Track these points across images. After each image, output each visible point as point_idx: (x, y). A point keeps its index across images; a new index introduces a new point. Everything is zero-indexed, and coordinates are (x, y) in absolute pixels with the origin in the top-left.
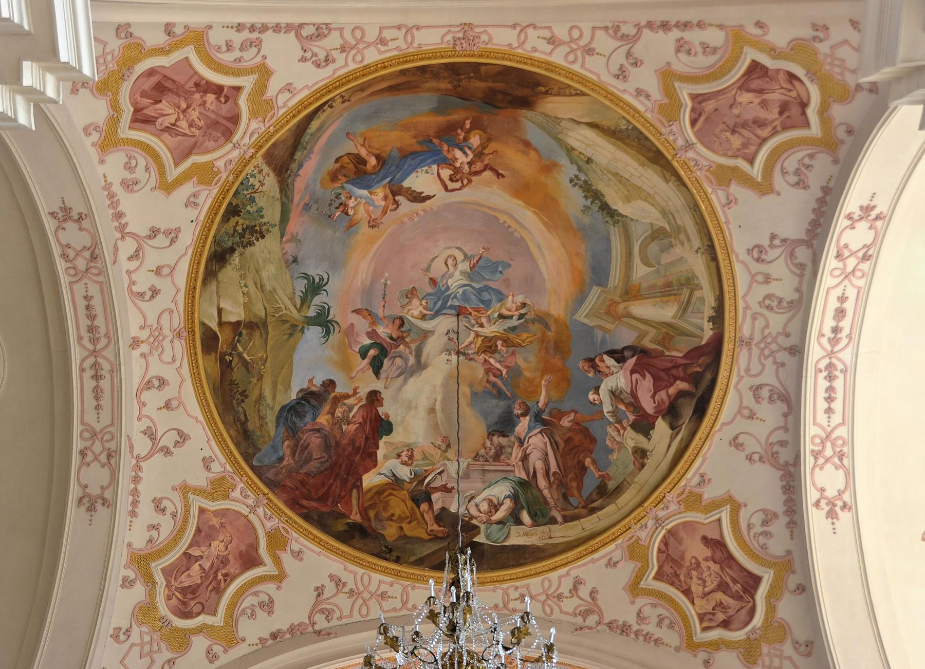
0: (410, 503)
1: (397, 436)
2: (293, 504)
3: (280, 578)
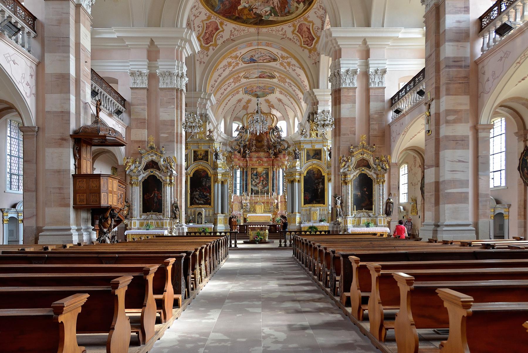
0: (248, 11)
2: (224, 16)
3: (223, 31)
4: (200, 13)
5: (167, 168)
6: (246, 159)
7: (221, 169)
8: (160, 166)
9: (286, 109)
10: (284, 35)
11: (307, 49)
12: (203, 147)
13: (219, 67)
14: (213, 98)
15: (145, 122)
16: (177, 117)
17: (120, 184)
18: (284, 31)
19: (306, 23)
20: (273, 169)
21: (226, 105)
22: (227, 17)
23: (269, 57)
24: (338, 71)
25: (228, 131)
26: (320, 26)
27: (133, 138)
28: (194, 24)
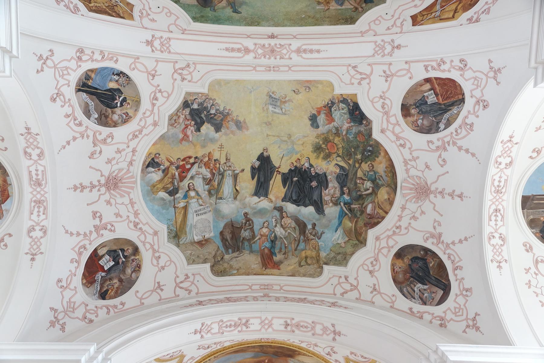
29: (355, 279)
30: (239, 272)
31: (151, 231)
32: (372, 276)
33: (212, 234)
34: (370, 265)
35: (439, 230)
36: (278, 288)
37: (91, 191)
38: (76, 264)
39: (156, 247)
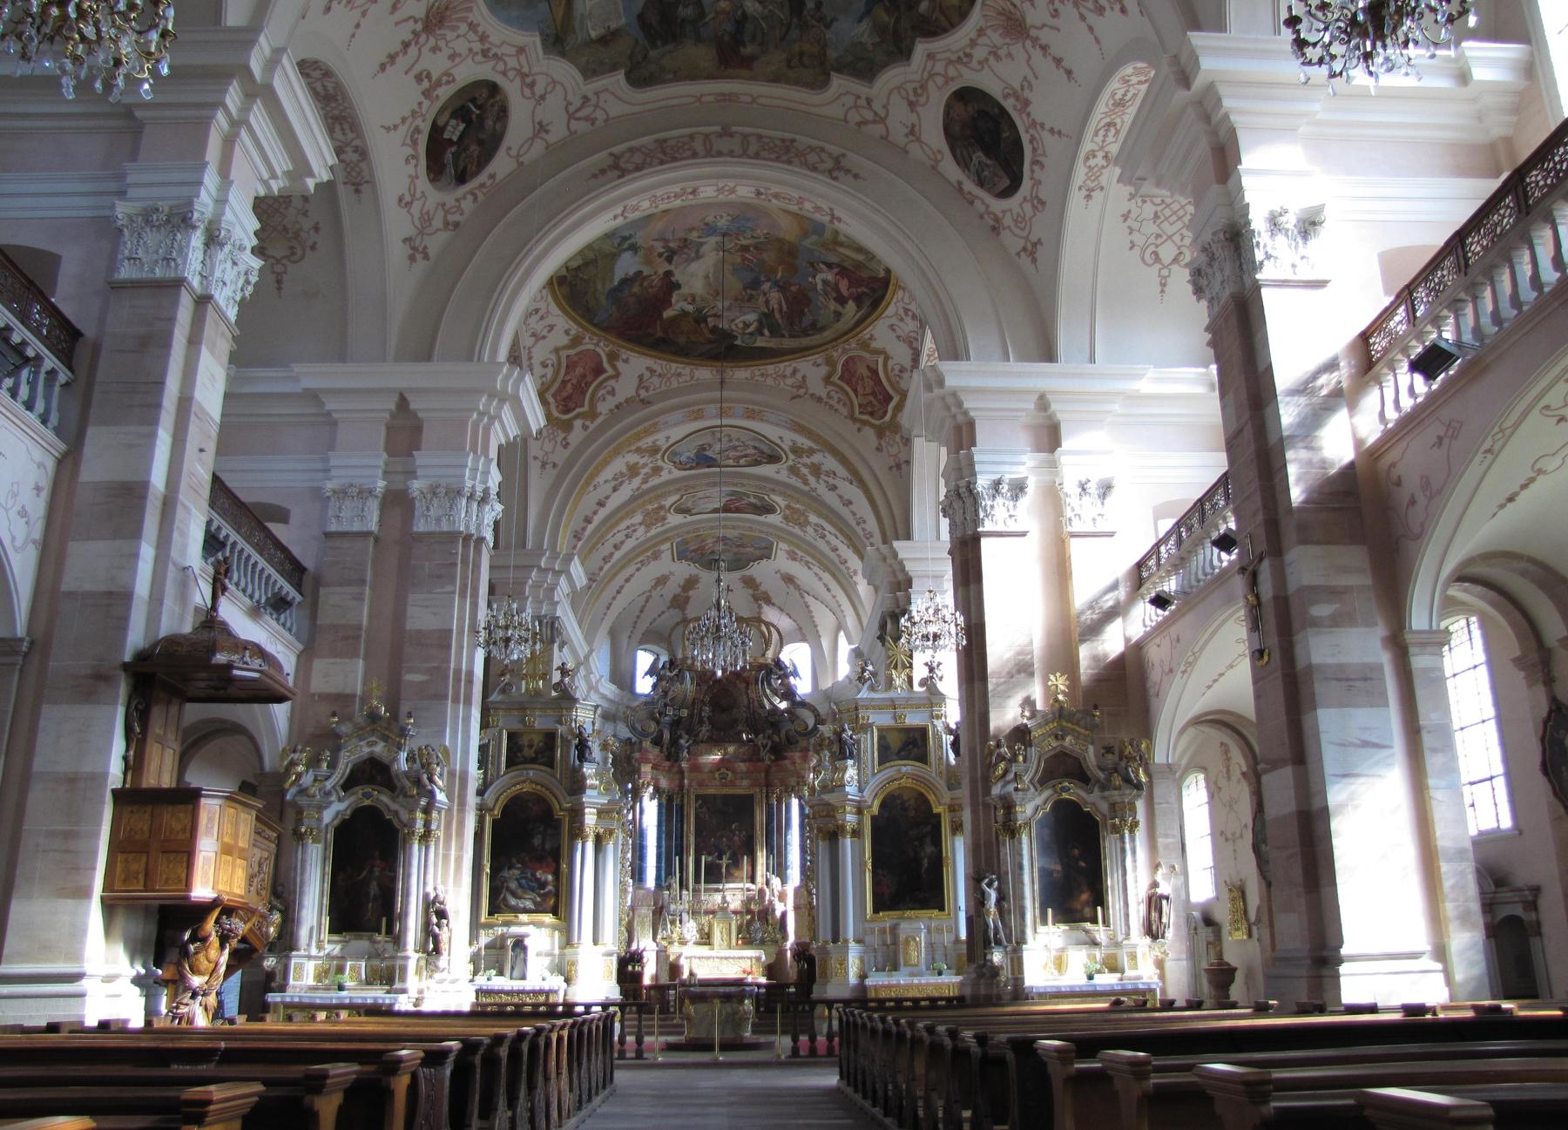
1: (684, 290)
3: (617, 376)
4: (551, 327)
5: (418, 782)
6: (680, 766)
7: (594, 793)
8: (397, 776)
9: (808, 607)
10: (799, 387)
11: (872, 425)
12: (540, 722)
13: (601, 479)
14: (577, 570)
15: (358, 637)
16: (461, 619)
17: (259, 825)
18: (799, 376)
19: (867, 355)
20: (767, 796)
21: (618, 592)
22: (629, 340)
23: (753, 451)
24: (969, 482)
25: (621, 677)
26: (908, 364)
27: (318, 684)
28: (530, 358)
29: (884, 107)
30: (679, 76)
31: (513, 51)
32: (912, 111)
33: (623, 21)
34: (911, 93)
35: (1027, 94)
36: (749, 99)
37: (405, 53)
38: (413, 162)
39: (526, 70)
